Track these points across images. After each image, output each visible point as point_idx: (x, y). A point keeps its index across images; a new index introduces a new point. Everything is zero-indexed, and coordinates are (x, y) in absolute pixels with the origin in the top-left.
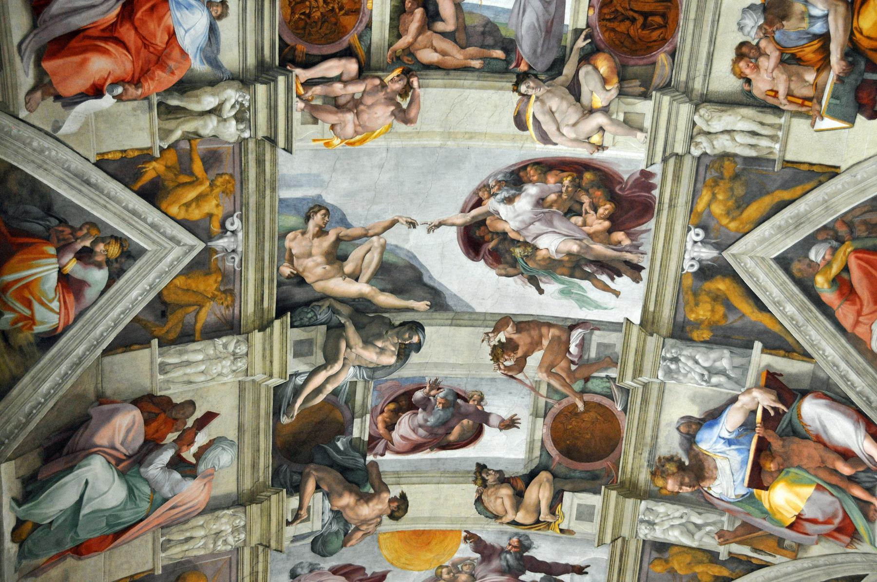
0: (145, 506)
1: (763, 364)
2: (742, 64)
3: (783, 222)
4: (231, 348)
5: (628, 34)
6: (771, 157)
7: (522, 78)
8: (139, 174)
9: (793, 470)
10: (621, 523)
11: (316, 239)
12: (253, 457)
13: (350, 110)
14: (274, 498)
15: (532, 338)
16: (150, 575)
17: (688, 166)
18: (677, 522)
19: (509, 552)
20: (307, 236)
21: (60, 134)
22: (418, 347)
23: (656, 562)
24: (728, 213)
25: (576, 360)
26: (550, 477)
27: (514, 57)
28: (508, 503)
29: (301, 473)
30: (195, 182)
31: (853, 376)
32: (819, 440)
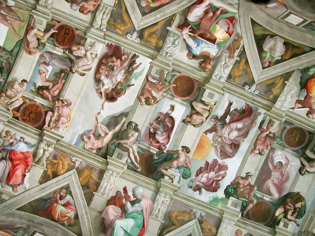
0: (140, 216)
1: (175, 29)
2: (85, 12)
3: (132, 11)
4: (108, 175)
5: (69, 40)
6: (112, 10)
7: (71, 70)
8: (49, 176)
9: (211, 29)
10: (217, 86)
11: (90, 140)
12: (145, 183)
13: (60, 118)
14: (161, 183)
15: (147, 92)
16: (162, 225)
17: (108, 33)
18: (222, 69)
19: (216, 123)
20: (88, 142)
21: (27, 189)
22: (137, 125)
23: (234, 80)
24: (125, 26)
25: (158, 82)
26: (195, 102)
27: (65, 71)
28: (199, 117)
29: (159, 172)
30: (58, 164)
31: (182, 4)
32: (201, 19)
